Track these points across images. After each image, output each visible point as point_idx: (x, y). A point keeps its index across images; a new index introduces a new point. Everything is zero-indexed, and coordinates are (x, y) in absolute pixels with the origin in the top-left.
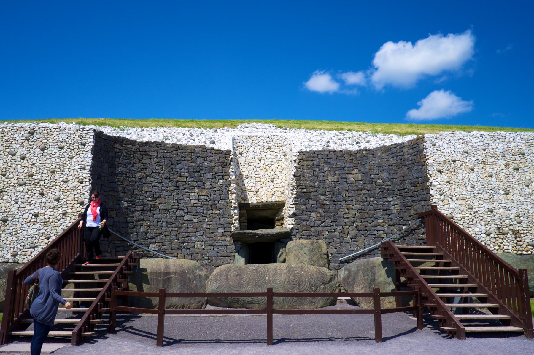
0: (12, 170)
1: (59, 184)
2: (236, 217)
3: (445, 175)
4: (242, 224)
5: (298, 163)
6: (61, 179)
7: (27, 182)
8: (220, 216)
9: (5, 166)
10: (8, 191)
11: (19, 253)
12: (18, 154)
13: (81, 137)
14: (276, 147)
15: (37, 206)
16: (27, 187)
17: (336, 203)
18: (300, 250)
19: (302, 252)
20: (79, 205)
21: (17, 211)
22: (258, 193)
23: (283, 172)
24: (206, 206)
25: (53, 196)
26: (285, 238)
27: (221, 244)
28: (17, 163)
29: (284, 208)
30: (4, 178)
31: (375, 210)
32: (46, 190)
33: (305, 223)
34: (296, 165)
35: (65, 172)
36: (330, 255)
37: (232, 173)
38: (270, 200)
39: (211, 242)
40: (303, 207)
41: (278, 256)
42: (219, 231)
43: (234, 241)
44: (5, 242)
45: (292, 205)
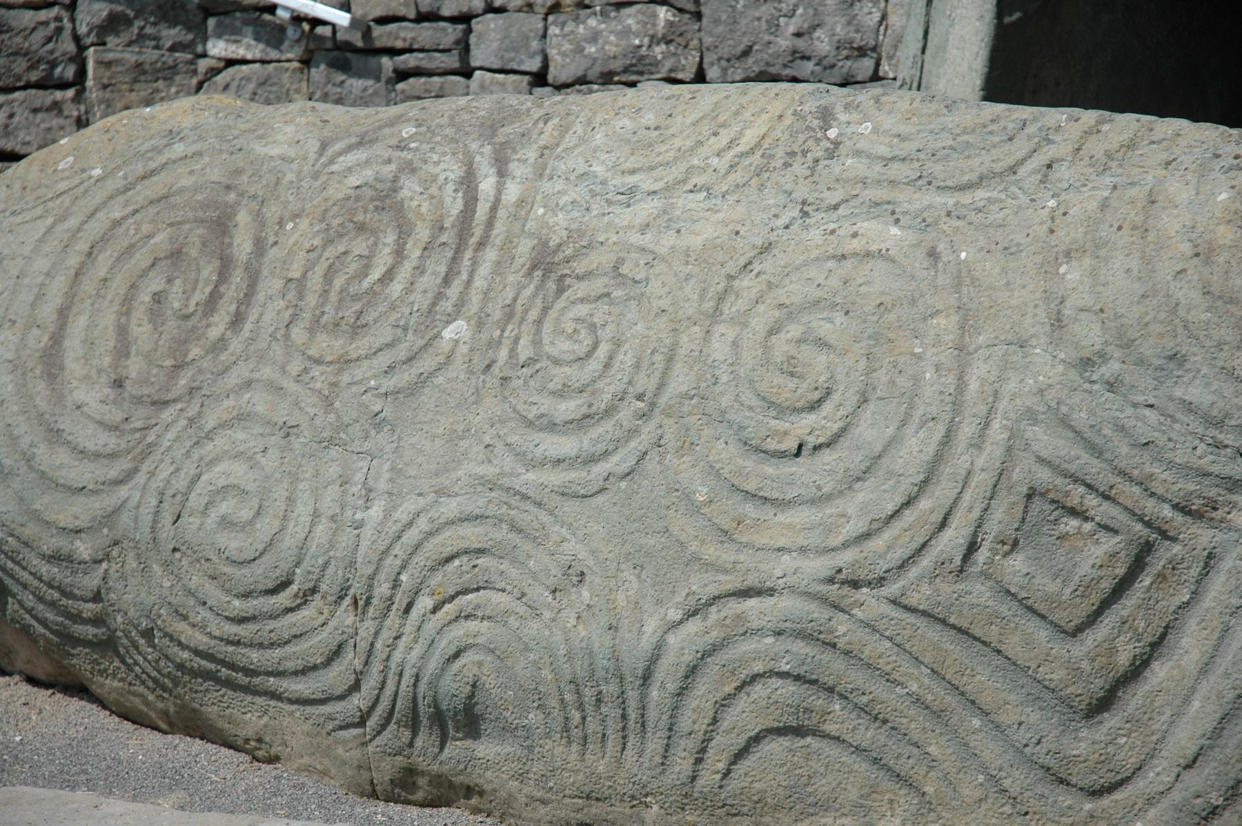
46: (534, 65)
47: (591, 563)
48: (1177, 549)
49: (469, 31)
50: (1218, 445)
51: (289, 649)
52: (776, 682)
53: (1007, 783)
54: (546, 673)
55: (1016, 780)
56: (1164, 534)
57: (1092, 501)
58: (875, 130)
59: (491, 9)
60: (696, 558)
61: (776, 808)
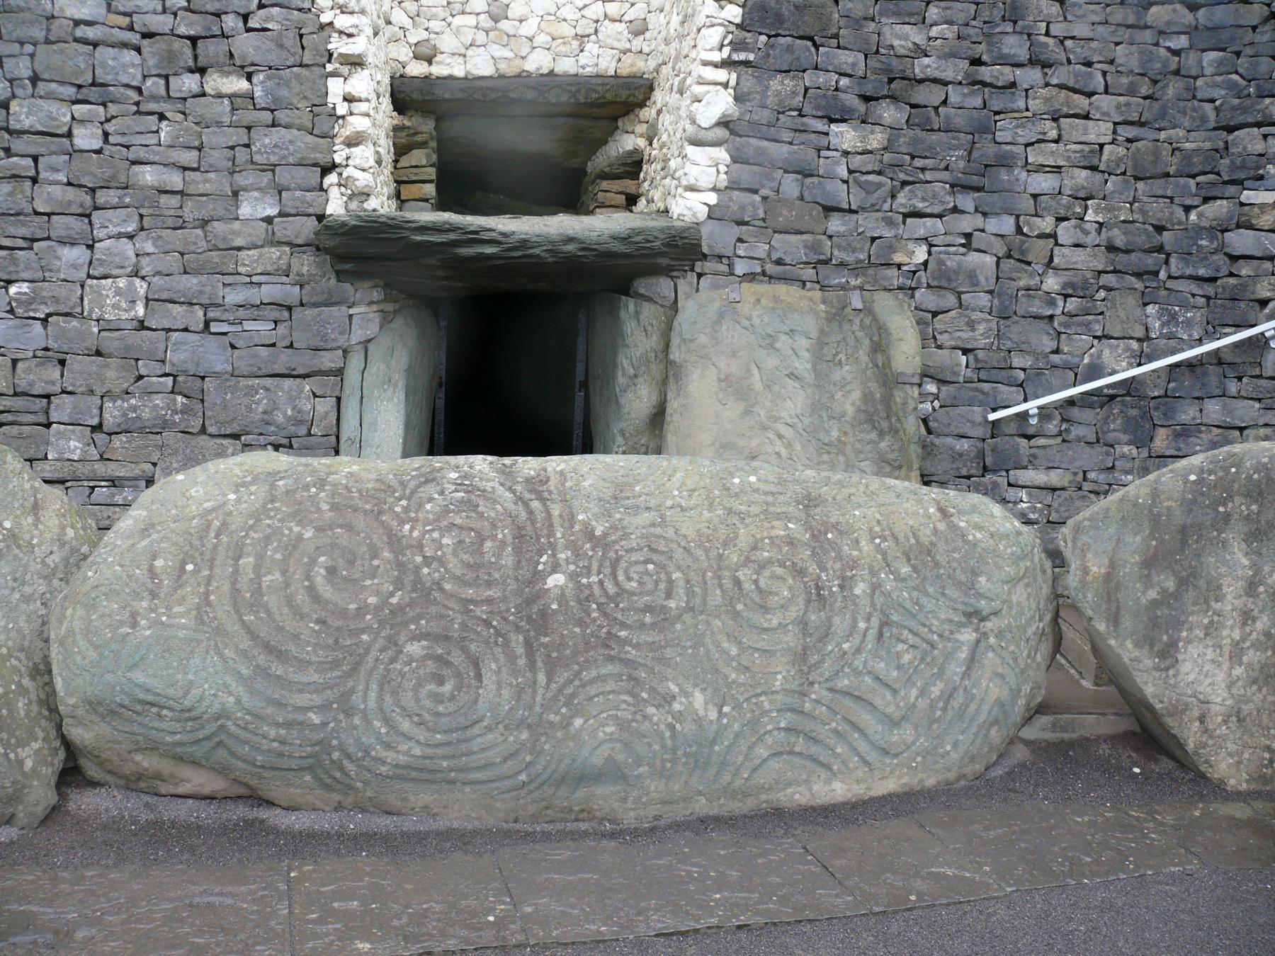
2: (358, 123)
4: (406, 192)
8: (250, 116)
17: (985, 73)
18: (762, 354)
19: (771, 362)
22: (504, 25)
24: (159, 44)
26: (666, 271)
27: (254, 296)
29: (647, 113)
31: (1230, 129)
33: (790, 186)
36: (931, 388)
38: (566, 66)
39: (191, 283)
40: (780, 86)
41: (621, 380)
42: (245, 210)
43: (340, 275)
45: (716, 66)
46: (95, 422)
47: (677, 690)
48: (936, 652)
49: (49, 403)
50: (955, 609)
51: (474, 757)
52: (776, 733)
53: (868, 758)
54: (656, 747)
55: (872, 756)
56: (933, 647)
57: (910, 636)
58: (759, 480)
59: (64, 392)
60: (734, 682)
61: (771, 788)
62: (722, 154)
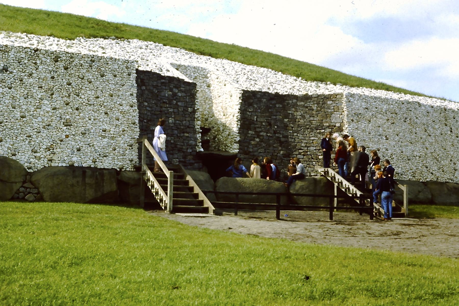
0: (83, 92)
1: (117, 107)
3: (355, 123)
5: (242, 100)
6: (118, 103)
7: (95, 103)
9: (78, 87)
10: (83, 109)
11: (97, 160)
12: (85, 78)
13: (127, 68)
14: (200, 78)
15: (104, 123)
16: (95, 107)
20: (132, 125)
21: (91, 127)
23: (207, 101)
25: (115, 116)
28: (85, 86)
30: (78, 98)
32: (108, 111)
34: (241, 101)
35: (120, 97)
37: (197, 103)
44: (86, 151)
62: (238, 145)
